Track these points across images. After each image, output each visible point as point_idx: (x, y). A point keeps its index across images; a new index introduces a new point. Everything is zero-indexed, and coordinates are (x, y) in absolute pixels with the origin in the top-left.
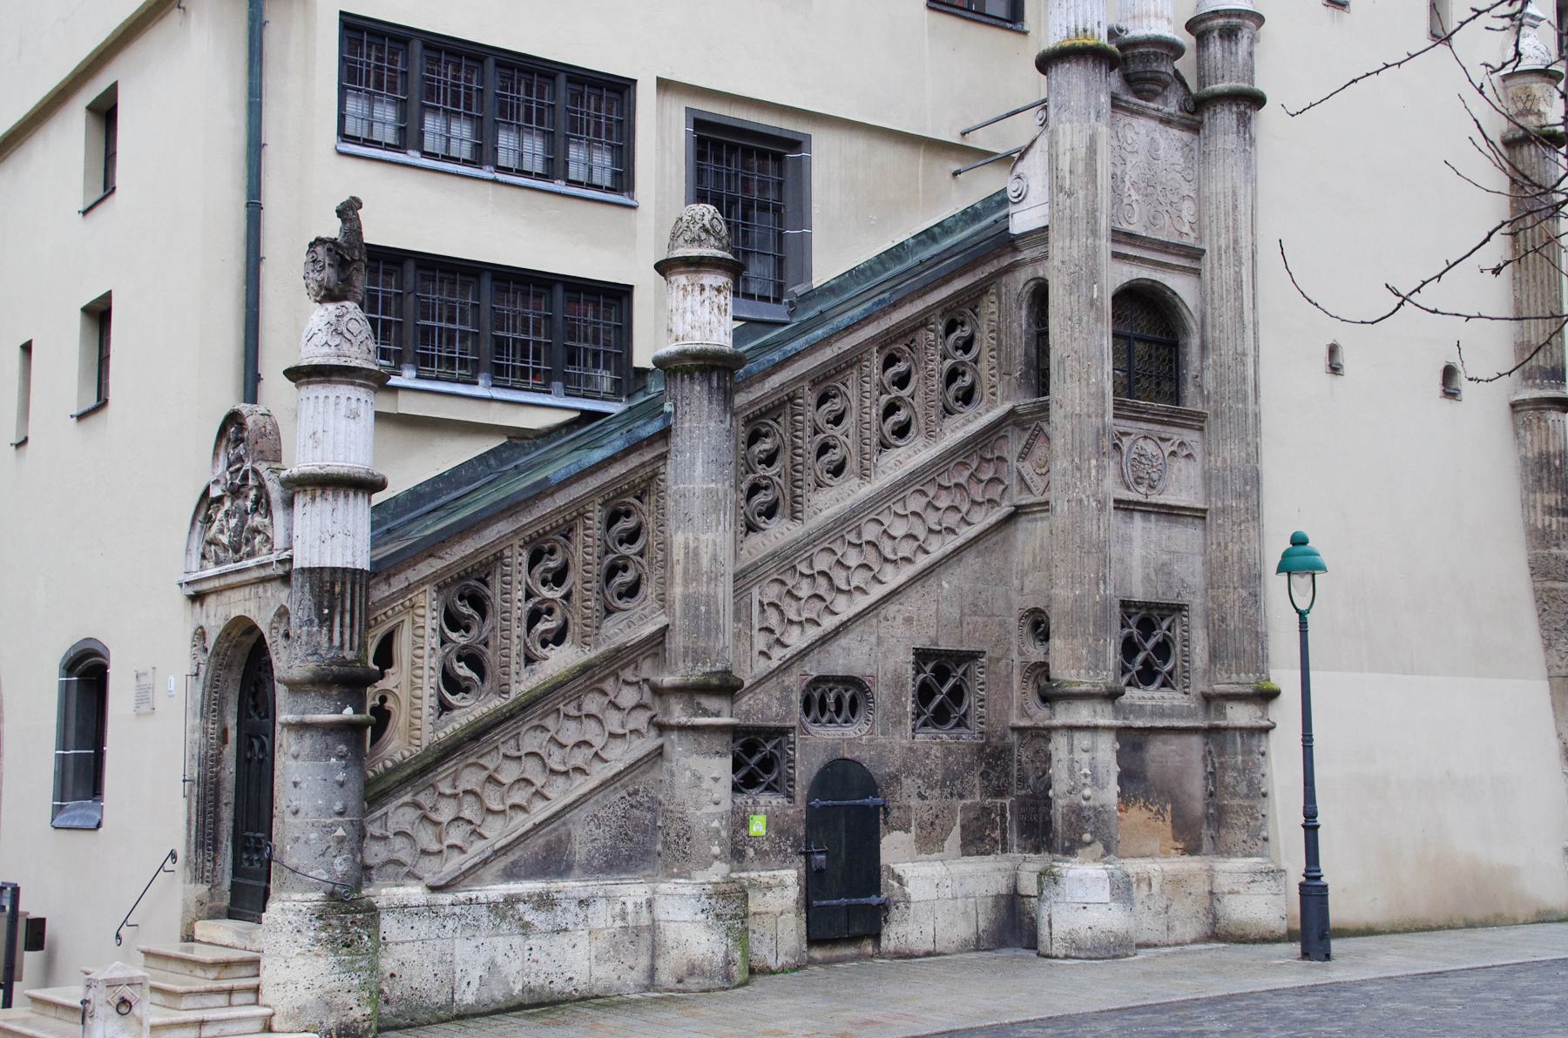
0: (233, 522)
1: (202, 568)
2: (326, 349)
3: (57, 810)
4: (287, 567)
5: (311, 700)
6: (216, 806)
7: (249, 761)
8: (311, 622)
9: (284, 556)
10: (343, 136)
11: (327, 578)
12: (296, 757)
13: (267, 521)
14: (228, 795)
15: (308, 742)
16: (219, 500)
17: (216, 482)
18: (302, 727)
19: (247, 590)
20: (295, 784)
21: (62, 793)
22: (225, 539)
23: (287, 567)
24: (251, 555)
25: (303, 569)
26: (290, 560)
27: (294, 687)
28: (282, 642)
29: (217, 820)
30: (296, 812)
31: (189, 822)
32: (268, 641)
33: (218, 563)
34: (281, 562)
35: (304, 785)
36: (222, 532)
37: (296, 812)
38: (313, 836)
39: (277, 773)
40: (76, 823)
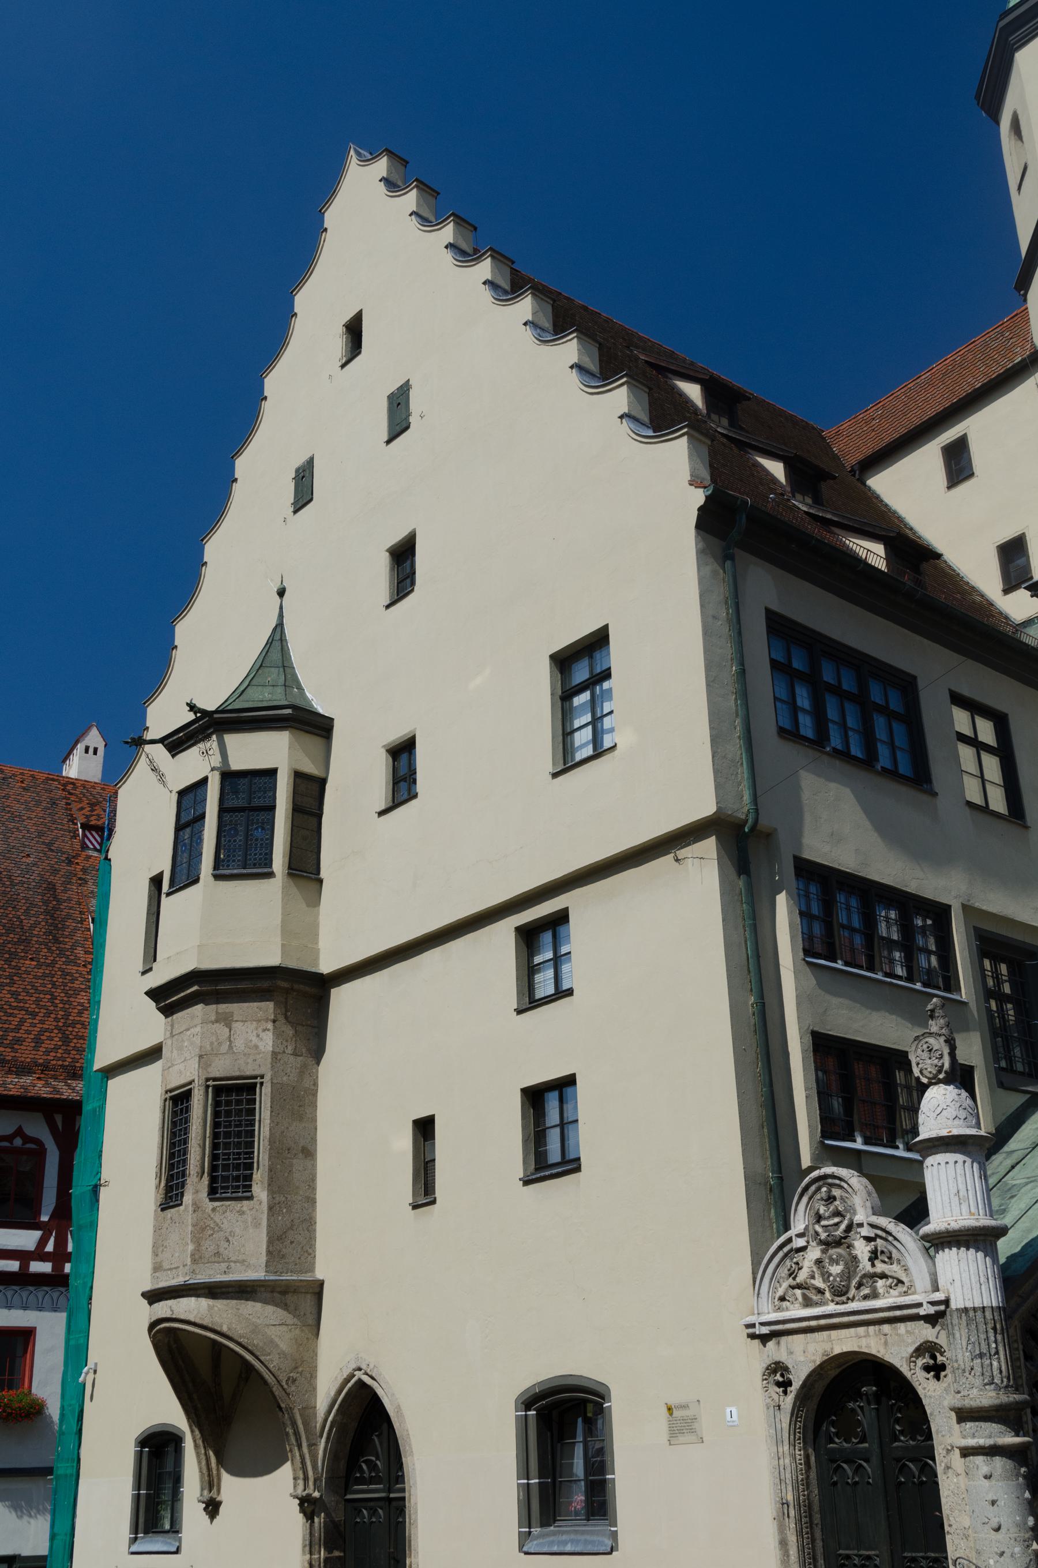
0: (836, 1269)
1: (779, 1309)
2: (957, 1122)
3: (524, 1538)
4: (942, 1308)
5: (994, 1427)
6: (811, 1528)
7: (835, 1484)
8: (981, 1355)
9: (939, 1296)
10: (807, 952)
11: (988, 1314)
12: (988, 1477)
13: (895, 1267)
14: (817, 1518)
15: (999, 1463)
16: (803, 1249)
17: (800, 1235)
18: (992, 1451)
19: (861, 1330)
20: (993, 1503)
21: (526, 1519)
22: (818, 1282)
23: (942, 1308)
24: (874, 1295)
25: (966, 1310)
26: (946, 1302)
27: (964, 1415)
28: (921, 1375)
29: (813, 1541)
30: (998, 1529)
31: (783, 1543)
32: (908, 1374)
33: (808, 1303)
34: (932, 1303)
35: (1001, 1503)
36: (813, 1277)
37: (998, 1529)
38: (1017, 1550)
39: (944, 1493)
40: (569, 1548)
